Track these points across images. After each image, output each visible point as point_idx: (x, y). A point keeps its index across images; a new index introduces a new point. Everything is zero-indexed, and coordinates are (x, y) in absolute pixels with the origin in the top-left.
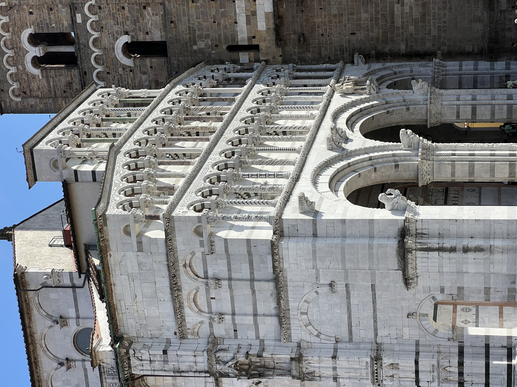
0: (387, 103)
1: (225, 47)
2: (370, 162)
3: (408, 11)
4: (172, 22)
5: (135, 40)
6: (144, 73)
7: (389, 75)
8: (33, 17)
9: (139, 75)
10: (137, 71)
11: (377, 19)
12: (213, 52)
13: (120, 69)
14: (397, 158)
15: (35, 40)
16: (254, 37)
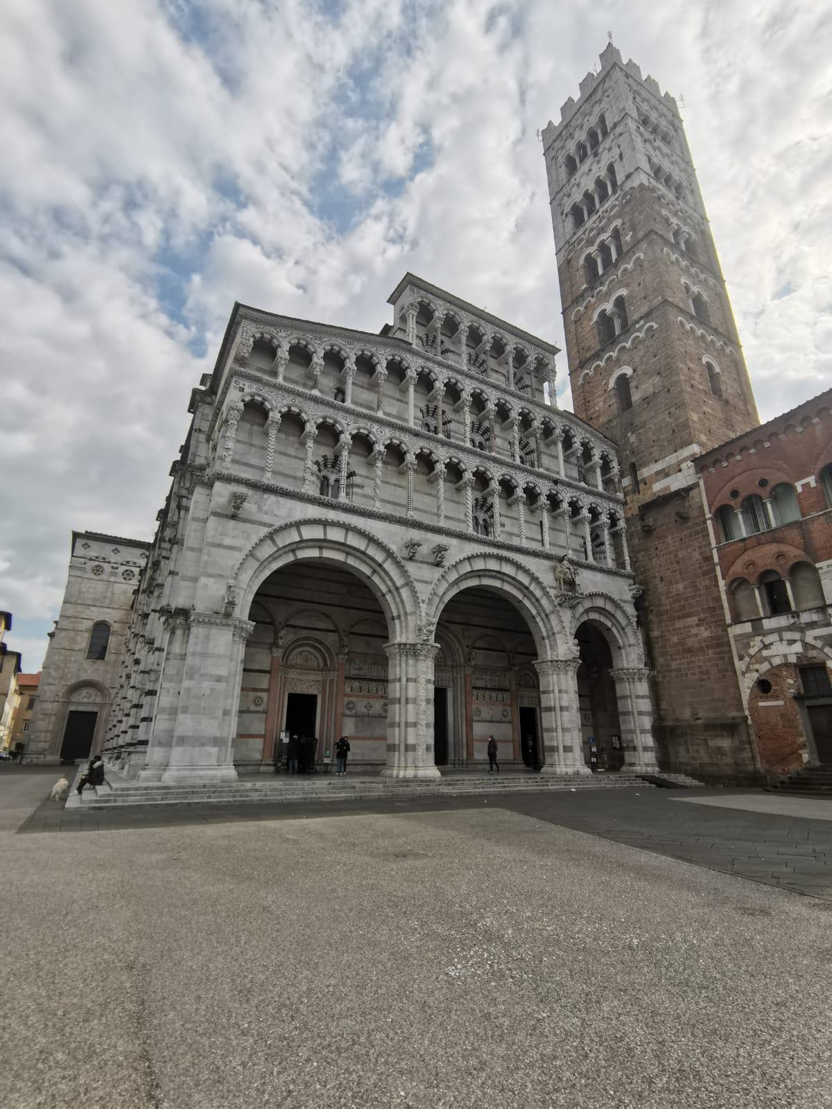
0: (547, 616)
1: (633, 460)
2: (393, 589)
3: (692, 632)
4: (648, 403)
5: (630, 380)
6: (604, 402)
7: (619, 622)
8: (637, 288)
9: (602, 399)
10: (606, 395)
11: (679, 601)
12: (628, 452)
13: (605, 382)
14: (403, 618)
15: (620, 302)
16: (645, 484)
